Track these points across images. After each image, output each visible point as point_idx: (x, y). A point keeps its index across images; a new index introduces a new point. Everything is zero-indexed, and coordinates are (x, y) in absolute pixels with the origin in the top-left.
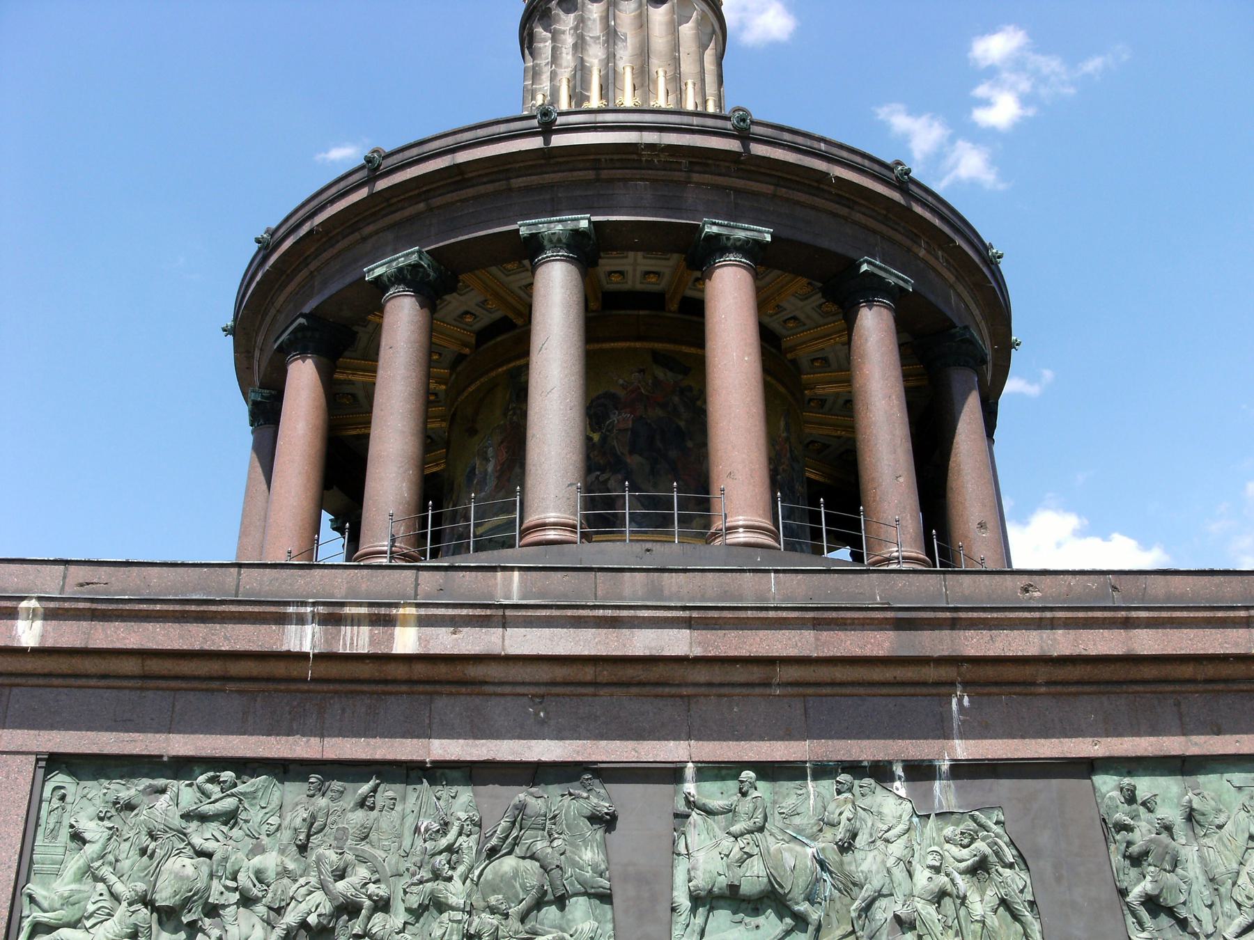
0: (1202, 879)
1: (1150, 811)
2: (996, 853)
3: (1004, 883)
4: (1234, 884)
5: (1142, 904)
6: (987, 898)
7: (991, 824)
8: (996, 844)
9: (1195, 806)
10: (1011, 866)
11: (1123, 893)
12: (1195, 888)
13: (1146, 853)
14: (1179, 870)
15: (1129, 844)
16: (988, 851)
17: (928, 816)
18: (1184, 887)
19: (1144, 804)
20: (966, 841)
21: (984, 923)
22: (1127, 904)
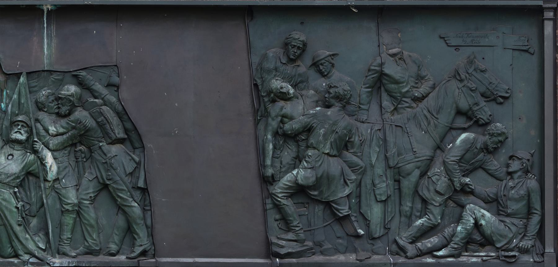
0: (379, 170)
1: (323, 75)
2: (101, 125)
3: (108, 166)
4: (423, 175)
5: (291, 196)
6: (84, 182)
7: (98, 87)
8: (101, 114)
9: (387, 70)
10: (120, 141)
11: (268, 181)
12: (367, 180)
13: (308, 130)
14: (349, 156)
15: (285, 118)
16: (90, 122)
17: (18, 75)
18: (353, 177)
19: (315, 65)
20: (64, 110)
21: (78, 213)
22: (271, 196)
